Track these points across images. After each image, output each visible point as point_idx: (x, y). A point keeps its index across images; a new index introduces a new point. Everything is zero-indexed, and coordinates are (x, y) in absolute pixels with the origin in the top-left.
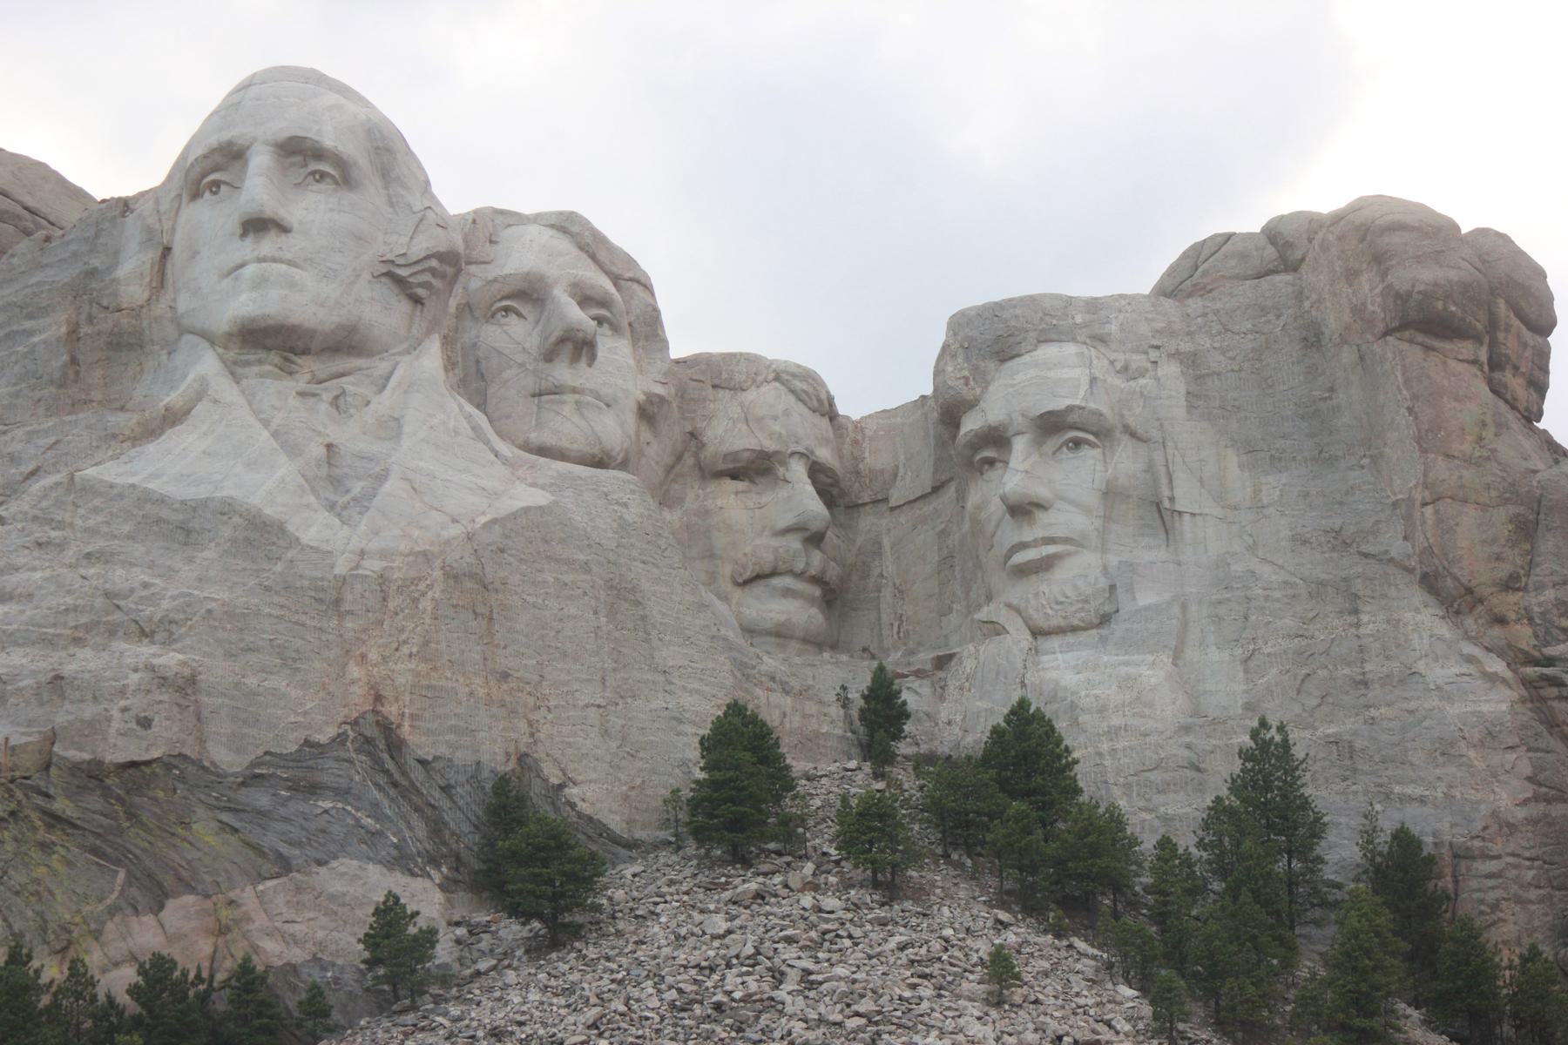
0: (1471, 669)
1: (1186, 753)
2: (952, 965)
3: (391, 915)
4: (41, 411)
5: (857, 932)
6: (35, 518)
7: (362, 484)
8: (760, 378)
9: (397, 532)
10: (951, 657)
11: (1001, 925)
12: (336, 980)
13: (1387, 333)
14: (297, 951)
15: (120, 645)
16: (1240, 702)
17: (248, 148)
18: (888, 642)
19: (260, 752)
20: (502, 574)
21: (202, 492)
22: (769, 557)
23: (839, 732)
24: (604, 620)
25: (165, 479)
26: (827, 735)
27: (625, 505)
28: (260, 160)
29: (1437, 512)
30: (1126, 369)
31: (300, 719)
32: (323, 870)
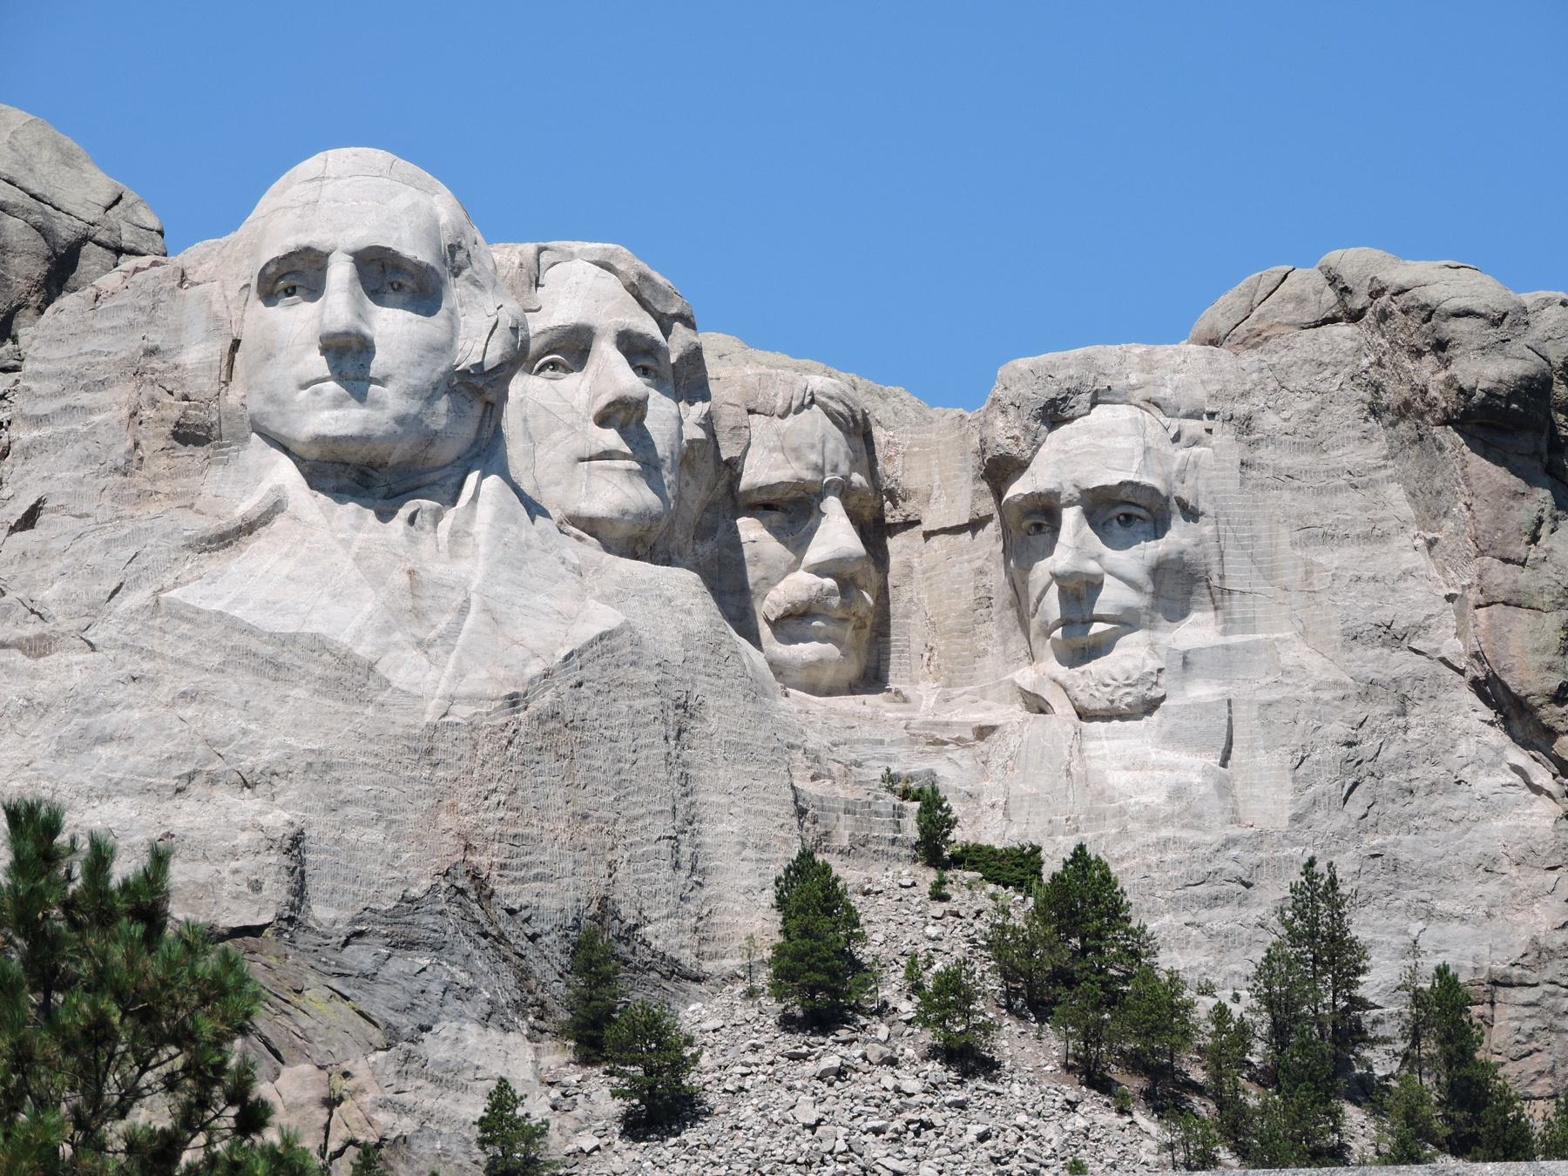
0: (1517, 779)
1: (1231, 866)
2: (1030, 1161)
3: (503, 1098)
4: (106, 502)
5: (938, 1122)
6: (124, 646)
7: (448, 618)
8: (795, 404)
9: (484, 674)
10: (993, 729)
11: (1072, 1106)
12: (445, 1152)
13: (1445, 422)
14: (406, 1120)
15: (224, 796)
16: (1288, 813)
17: (328, 255)
18: (918, 673)
19: (360, 909)
20: (582, 709)
21: (286, 624)
22: (805, 597)
23: (890, 835)
24: (673, 743)
25: (251, 604)
26: (879, 839)
27: (689, 612)
28: (340, 272)
29: (1490, 616)
30: (1176, 438)
31: (396, 874)
32: (424, 1035)
